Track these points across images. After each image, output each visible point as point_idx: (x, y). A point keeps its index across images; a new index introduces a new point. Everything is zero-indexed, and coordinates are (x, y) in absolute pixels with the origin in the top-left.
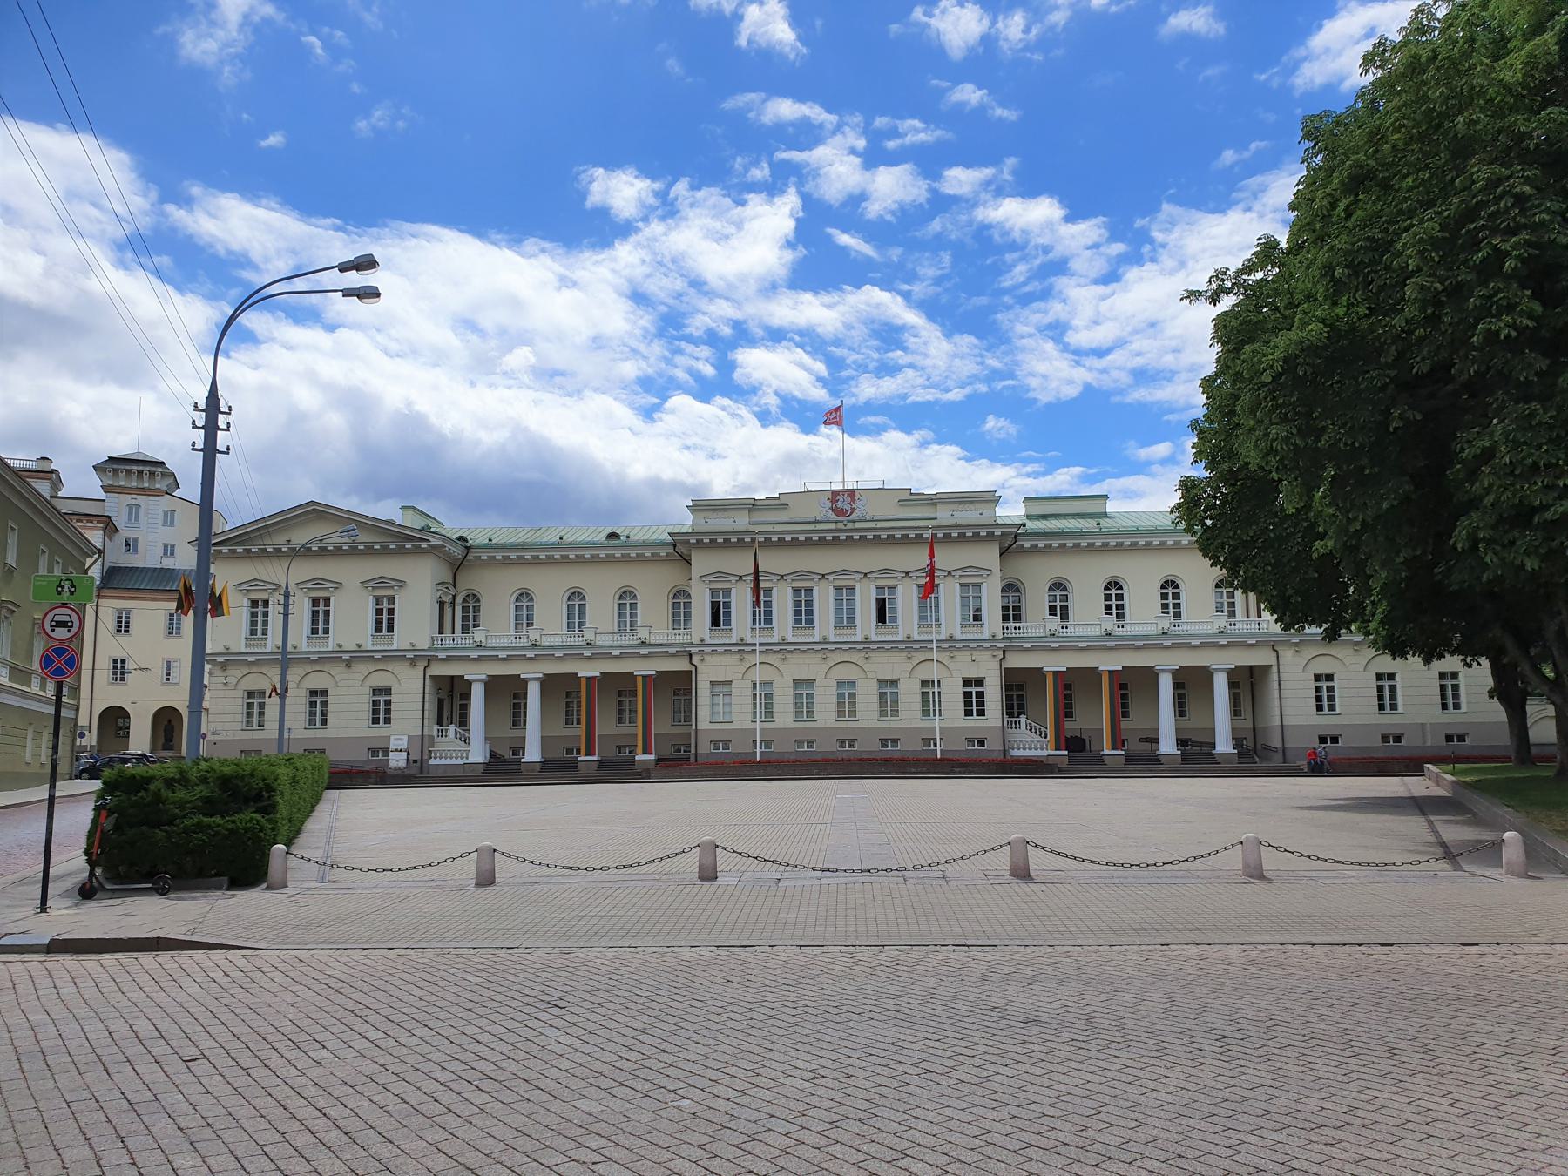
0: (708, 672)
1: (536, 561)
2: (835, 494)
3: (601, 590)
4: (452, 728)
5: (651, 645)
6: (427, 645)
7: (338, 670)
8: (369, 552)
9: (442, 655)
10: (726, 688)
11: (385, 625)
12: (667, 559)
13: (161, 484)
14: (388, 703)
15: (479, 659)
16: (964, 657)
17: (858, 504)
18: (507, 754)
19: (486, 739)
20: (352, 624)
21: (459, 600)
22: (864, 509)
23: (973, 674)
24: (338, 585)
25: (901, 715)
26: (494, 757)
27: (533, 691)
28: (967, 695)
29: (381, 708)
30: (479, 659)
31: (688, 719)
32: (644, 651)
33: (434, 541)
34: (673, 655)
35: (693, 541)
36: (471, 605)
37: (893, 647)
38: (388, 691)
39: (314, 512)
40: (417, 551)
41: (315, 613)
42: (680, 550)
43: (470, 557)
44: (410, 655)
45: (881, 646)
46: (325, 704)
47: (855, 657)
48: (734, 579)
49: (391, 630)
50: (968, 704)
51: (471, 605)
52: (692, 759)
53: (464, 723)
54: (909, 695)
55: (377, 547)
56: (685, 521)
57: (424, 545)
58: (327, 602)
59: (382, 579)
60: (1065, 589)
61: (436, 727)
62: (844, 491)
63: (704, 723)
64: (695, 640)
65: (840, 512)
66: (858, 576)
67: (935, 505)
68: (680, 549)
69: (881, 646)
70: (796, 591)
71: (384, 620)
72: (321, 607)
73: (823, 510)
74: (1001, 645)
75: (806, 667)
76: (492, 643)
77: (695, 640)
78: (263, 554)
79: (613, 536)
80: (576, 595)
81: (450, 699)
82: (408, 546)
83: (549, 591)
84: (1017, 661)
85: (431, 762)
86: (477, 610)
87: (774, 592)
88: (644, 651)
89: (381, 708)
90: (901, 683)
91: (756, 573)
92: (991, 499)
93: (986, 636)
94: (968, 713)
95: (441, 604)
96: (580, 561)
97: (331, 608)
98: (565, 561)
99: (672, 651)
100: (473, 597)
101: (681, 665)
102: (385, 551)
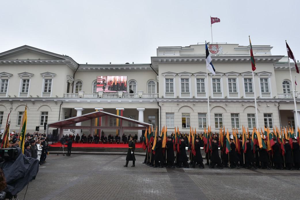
0: (165, 109)
5: (143, 98)
6: (62, 96)
7: (30, 105)
10: (172, 116)
12: (147, 71)
16: (264, 105)
17: (220, 49)
20: (36, 89)
21: (75, 83)
23: (268, 112)
24: (33, 75)
28: (265, 120)
32: (141, 101)
33: (67, 60)
37: (237, 101)
38: (47, 113)
41: (24, 85)
43: (80, 68)
44: (55, 100)
45: (232, 101)
48: (174, 75)
49: (50, 91)
50: (266, 123)
51: (79, 85)
54: (243, 120)
57: (63, 61)
58: (28, 81)
59: (48, 73)
60: (288, 83)
66: (222, 75)
68: (154, 66)
69: (232, 101)
71: (47, 89)
72: (26, 83)
74: (278, 101)
75: (200, 108)
76: (85, 96)
77: (159, 97)
78: (8, 64)
82: (58, 61)
84: (284, 107)
88: (141, 101)
90: (240, 114)
93: (272, 97)
95: (69, 84)
97: (30, 83)
100: (80, 82)
101: (155, 106)
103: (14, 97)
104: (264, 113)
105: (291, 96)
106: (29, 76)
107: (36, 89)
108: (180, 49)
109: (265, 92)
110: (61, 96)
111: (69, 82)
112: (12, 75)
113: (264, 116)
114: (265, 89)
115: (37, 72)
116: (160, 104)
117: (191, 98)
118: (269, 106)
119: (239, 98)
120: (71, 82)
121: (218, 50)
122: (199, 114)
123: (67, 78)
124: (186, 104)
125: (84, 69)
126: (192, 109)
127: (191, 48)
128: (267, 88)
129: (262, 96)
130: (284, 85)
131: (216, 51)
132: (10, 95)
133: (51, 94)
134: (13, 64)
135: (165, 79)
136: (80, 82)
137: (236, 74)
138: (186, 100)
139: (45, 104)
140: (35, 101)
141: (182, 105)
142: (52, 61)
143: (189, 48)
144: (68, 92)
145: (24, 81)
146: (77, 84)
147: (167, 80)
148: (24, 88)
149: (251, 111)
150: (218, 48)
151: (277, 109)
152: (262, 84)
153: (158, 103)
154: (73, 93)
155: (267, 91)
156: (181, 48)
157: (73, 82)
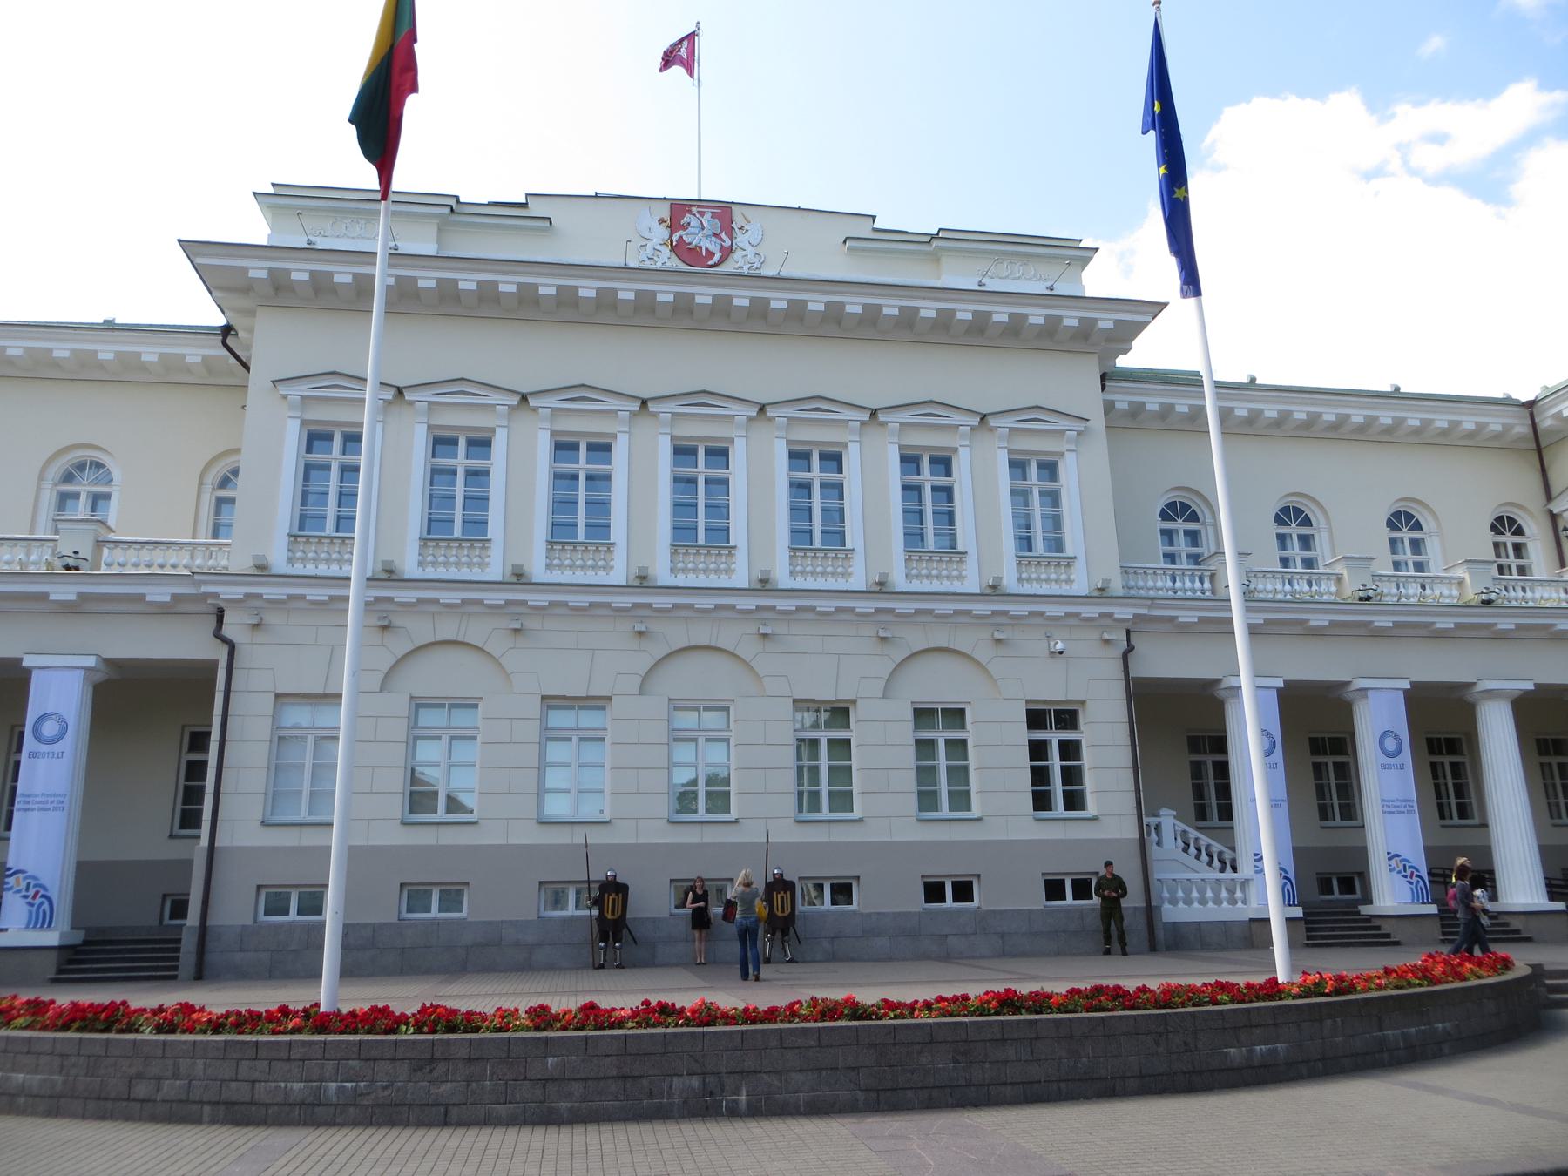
0: (265, 670)
2: (679, 210)
17: (741, 239)
22: (755, 251)
28: (1038, 750)
32: (64, 592)
47: (729, 635)
50: (1040, 776)
52: (188, 944)
60: (1194, 517)
62: (702, 204)
64: (239, 561)
65: (688, 253)
67: (935, 258)
69: (810, 610)
73: (648, 245)
74: (1125, 612)
84: (1166, 661)
92: (1076, 254)
94: (1042, 801)
99: (159, 594)
101: (185, 643)
104: (1028, 701)
105: (1207, 585)
108: (446, 211)
109: (1039, 547)
113: (1030, 727)
114: (1038, 533)
116: (227, 631)
117: (499, 579)
118: (1060, 646)
119: (858, 582)
121: (727, 243)
122: (551, 702)
127: (536, 209)
128: (1056, 522)
129: (1020, 580)
130: (1168, 525)
131: (711, 248)
135: (293, 436)
137: (847, 414)
138: (454, 597)
143: (515, 214)
147: (315, 438)
149: (939, 684)
150: (730, 232)
151: (1114, 669)
152: (1020, 496)
153: (220, 615)
155: (1057, 544)
156: (453, 202)
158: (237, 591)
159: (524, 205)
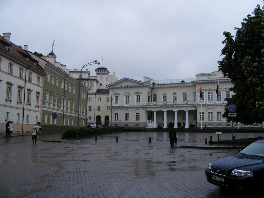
1: (167, 87)
3: (179, 93)
4: (151, 121)
7: (130, 110)
8: (135, 87)
9: (148, 107)
11: (138, 101)
12: (192, 86)
13: (106, 73)
14: (139, 116)
15: (155, 107)
18: (161, 126)
19: (157, 123)
25: (213, 119)
26: (158, 126)
27: (165, 114)
29: (138, 116)
30: (155, 107)
31: (195, 120)
33: (146, 84)
34: (192, 106)
35: (196, 82)
36: (155, 96)
39: (126, 80)
40: (144, 86)
41: (126, 99)
42: (194, 84)
43: (154, 87)
44: (142, 107)
46: (128, 116)
49: (139, 102)
51: (155, 96)
53: (152, 119)
55: (136, 86)
56: (194, 78)
61: (148, 121)
63: (198, 120)
64: (197, 103)
70: (209, 93)
71: (138, 100)
76: (158, 104)
77: (197, 103)
79: (183, 81)
80: (175, 94)
81: (150, 115)
82: (142, 85)
83: (170, 93)
85: (147, 127)
86: (156, 97)
87: (222, 92)
89: (138, 116)
91: (201, 89)
95: (149, 97)
96: (175, 87)
98: (172, 87)
99: (192, 106)
100: (155, 95)
101: (193, 109)
102: (138, 86)
103: (122, 106)
106: (128, 94)
107: (133, 101)
110: (145, 104)
111: (149, 95)
112: (120, 94)
115: (132, 91)
116: (196, 108)
120: (150, 95)
123: (148, 94)
124: (210, 107)
125: (157, 87)
126: (214, 110)
127: (215, 73)
132: (120, 104)
133: (140, 103)
134: (120, 88)
136: (156, 94)
139: (137, 109)
140: (134, 107)
141: (208, 107)
142: (139, 86)
144: (149, 101)
145: (126, 97)
146: (154, 96)
148: (126, 100)
154: (152, 102)
156: (208, 74)
157: (152, 95)
158: (196, 105)
159: (214, 73)
